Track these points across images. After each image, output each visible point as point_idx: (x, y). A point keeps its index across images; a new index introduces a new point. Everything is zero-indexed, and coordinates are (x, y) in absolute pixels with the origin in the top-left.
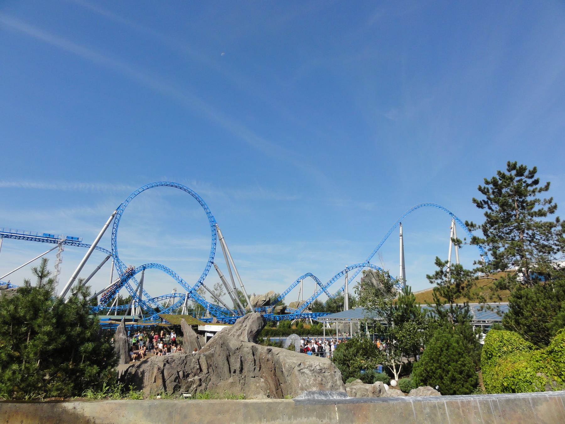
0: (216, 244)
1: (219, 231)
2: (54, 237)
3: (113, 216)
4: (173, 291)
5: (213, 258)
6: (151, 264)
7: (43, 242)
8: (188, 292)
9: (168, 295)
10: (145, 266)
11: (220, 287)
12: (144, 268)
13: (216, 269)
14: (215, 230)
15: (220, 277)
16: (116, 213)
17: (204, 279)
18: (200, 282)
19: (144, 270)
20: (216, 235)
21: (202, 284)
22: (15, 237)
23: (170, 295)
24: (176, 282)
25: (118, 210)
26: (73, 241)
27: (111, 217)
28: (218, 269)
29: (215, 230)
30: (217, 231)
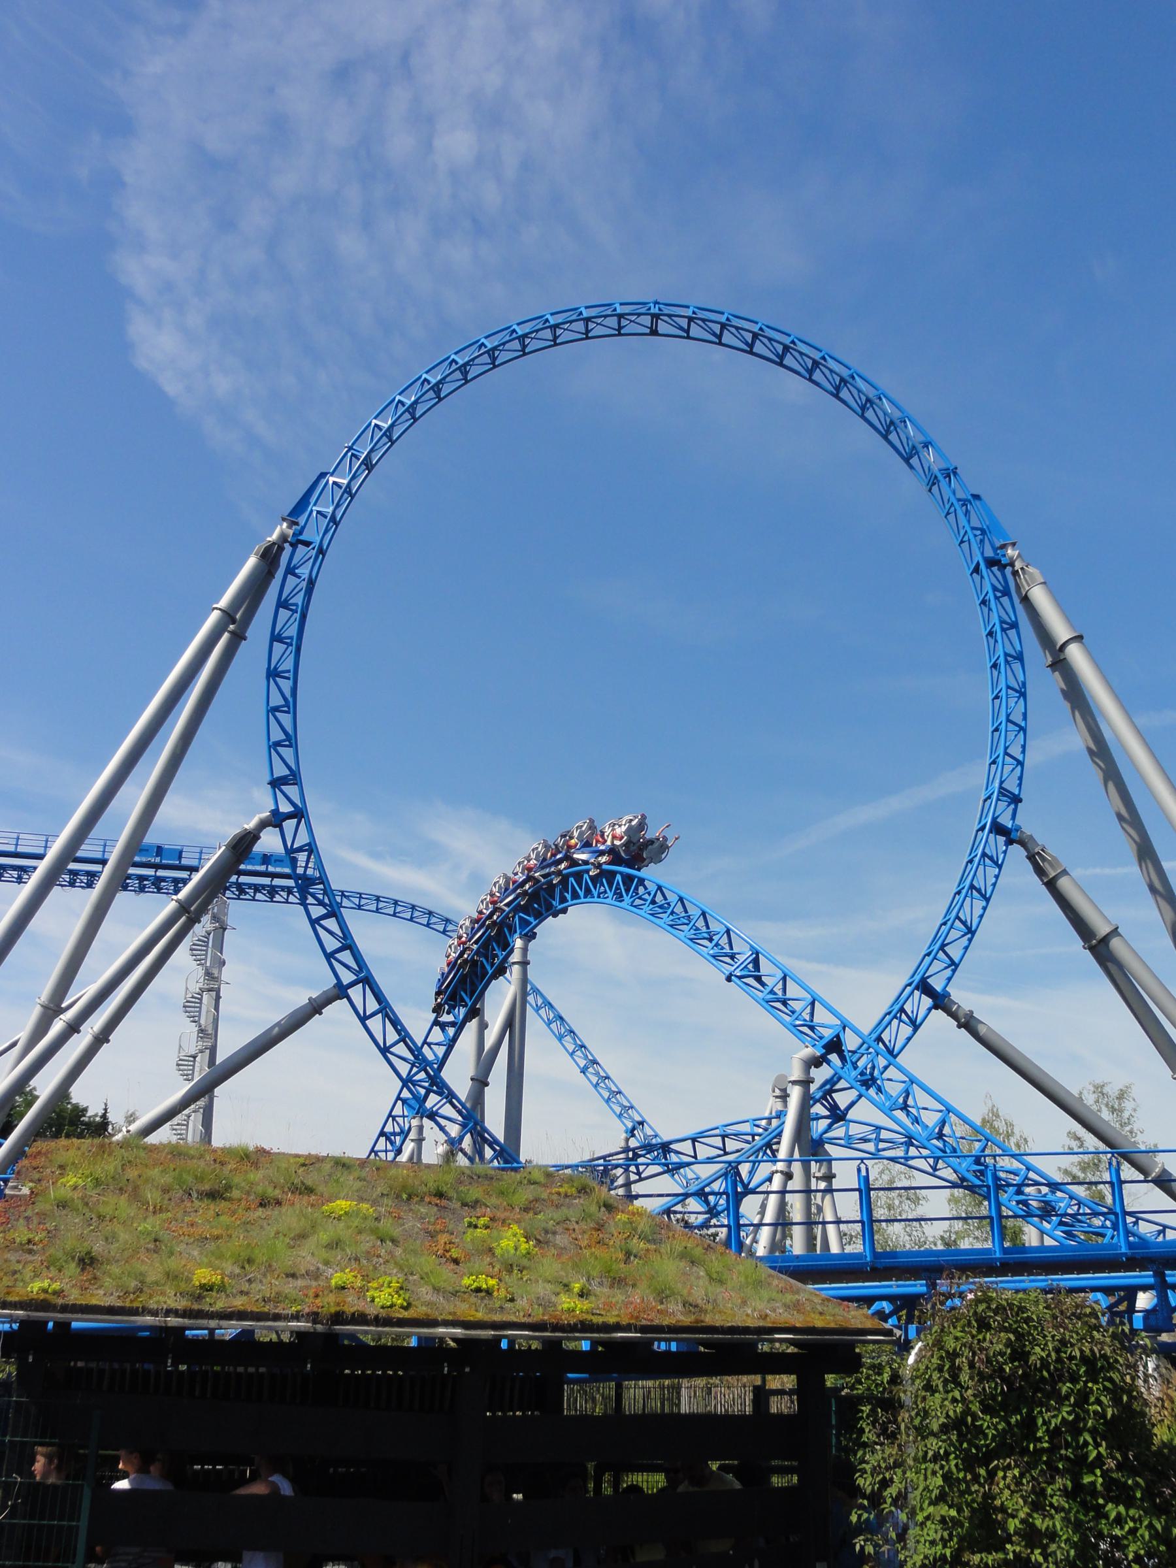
0: (1022, 694)
1: (1040, 596)
2: (184, 862)
3: (270, 557)
4: (772, 1100)
5: (1016, 800)
7: (142, 889)
8: (808, 1052)
11: (1113, 1110)
13: (1051, 885)
14: (1006, 592)
15: (1092, 949)
16: (283, 538)
17: (954, 965)
18: (925, 987)
20: (1014, 625)
21: (941, 1001)
22: (15, 874)
23: (746, 1128)
24: (712, 974)
25: (302, 520)
26: (274, 876)
27: (252, 561)
28: (1064, 884)
29: (1006, 592)
30: (1026, 600)
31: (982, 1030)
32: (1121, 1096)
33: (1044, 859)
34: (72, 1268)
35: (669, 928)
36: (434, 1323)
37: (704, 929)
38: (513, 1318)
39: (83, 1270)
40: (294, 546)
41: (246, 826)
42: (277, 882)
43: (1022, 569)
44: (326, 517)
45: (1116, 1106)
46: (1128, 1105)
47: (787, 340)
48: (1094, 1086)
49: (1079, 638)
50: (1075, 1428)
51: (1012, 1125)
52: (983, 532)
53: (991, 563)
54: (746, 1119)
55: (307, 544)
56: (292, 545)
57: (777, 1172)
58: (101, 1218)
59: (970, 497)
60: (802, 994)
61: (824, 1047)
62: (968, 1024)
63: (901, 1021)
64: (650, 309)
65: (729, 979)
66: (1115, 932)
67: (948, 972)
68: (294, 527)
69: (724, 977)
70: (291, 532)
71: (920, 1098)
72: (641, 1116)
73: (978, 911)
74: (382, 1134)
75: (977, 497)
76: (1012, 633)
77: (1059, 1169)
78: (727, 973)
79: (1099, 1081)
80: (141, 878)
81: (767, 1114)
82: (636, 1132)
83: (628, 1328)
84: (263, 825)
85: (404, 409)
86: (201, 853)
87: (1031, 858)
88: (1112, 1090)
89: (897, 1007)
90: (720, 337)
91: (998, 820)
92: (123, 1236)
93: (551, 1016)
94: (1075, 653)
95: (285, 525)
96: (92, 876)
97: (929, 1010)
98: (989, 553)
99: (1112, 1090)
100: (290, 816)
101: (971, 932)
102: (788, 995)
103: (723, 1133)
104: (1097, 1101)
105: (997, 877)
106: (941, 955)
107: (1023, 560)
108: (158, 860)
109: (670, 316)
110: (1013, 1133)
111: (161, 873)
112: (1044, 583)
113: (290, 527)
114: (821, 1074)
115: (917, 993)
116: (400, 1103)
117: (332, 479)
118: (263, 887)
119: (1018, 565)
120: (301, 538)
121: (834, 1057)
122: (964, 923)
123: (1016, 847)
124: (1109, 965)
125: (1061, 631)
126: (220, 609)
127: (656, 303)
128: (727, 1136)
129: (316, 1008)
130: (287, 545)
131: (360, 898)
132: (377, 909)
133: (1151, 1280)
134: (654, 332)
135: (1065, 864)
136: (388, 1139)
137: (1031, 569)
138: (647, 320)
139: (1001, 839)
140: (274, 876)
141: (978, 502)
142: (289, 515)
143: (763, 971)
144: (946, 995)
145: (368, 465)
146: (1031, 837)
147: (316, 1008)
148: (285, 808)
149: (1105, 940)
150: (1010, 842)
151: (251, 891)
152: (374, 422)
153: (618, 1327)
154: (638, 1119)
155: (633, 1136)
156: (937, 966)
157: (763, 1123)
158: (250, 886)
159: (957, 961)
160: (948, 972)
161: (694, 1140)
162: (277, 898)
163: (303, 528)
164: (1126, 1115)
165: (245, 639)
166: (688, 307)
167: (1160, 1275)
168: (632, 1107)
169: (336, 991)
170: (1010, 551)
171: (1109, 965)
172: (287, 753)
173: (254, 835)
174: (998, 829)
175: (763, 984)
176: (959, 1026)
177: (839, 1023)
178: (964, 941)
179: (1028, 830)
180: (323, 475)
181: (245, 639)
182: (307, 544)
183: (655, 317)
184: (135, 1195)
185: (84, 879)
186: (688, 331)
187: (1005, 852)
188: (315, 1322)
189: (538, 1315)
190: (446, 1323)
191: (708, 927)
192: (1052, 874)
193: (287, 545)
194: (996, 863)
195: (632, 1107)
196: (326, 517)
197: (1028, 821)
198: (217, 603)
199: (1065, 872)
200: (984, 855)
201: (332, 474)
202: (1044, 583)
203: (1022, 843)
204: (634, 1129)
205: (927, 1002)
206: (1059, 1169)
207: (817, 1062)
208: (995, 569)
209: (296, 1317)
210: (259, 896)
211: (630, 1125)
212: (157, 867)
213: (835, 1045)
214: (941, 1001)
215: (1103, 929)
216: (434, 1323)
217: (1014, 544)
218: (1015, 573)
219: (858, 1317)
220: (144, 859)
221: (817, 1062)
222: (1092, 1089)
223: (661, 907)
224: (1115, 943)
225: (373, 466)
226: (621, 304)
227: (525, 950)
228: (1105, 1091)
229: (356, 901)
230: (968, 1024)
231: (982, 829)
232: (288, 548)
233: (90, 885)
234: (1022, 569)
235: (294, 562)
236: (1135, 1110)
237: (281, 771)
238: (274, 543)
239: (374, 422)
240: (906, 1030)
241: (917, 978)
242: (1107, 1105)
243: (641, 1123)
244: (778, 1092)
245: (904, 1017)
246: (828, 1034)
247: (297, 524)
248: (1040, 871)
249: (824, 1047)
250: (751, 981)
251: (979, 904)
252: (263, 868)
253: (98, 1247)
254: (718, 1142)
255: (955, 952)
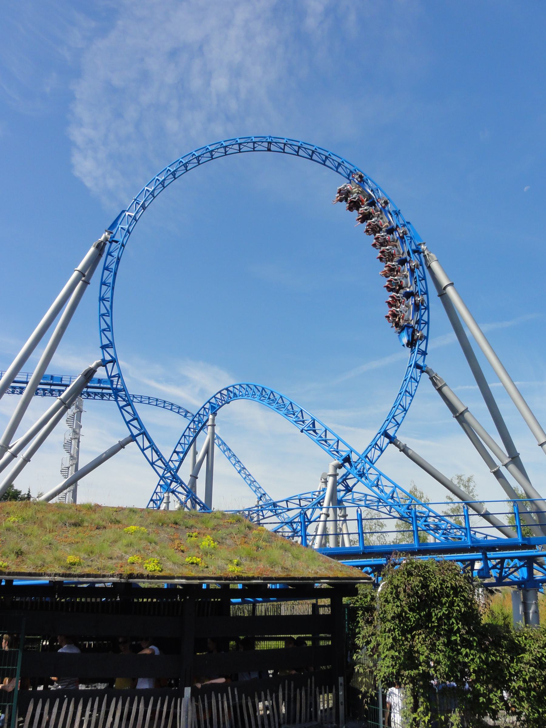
1: (435, 266)
2: (63, 382)
3: (100, 248)
4: (320, 483)
6: (227, 389)
7: (44, 395)
8: (336, 462)
9: (302, 497)
10: (213, 401)
11: (465, 486)
12: (214, 410)
13: (440, 390)
15: (457, 417)
16: (106, 239)
17: (398, 425)
18: (386, 435)
19: (215, 414)
20: (424, 279)
21: (392, 440)
23: (309, 496)
25: (114, 231)
26: (103, 388)
27: (92, 249)
28: (445, 390)
30: (429, 268)
31: (410, 452)
32: (469, 480)
33: (436, 379)
34: (13, 556)
35: (276, 410)
36: (173, 578)
37: (291, 410)
38: (208, 575)
39: (17, 557)
40: (111, 242)
41: (91, 366)
42: (104, 391)
43: (428, 254)
44: (125, 230)
45: (467, 485)
46: (472, 484)
47: (327, 154)
48: (458, 476)
49: (452, 284)
50: (448, 617)
51: (422, 493)
52: (411, 238)
53: (414, 252)
54: (309, 492)
55: (117, 242)
56: (110, 242)
57: (322, 514)
58: (26, 535)
59: (406, 223)
60: (334, 438)
61: (343, 460)
62: (404, 450)
63: (375, 449)
64: (267, 140)
65: (302, 431)
66: (466, 410)
67: (396, 428)
68: (111, 234)
69: (300, 430)
70: (109, 237)
71: (384, 482)
72: (264, 491)
73: (408, 401)
74: (152, 500)
75: (408, 223)
76: (423, 282)
77: (443, 512)
78: (301, 429)
79: (459, 474)
80: (44, 390)
81: (318, 490)
82: (262, 498)
83: (258, 578)
84: (98, 365)
85: (159, 183)
86: (71, 379)
87: (431, 379)
88: (465, 478)
89: (374, 443)
90: (298, 152)
91: (418, 362)
92: (36, 542)
93: (225, 449)
94: (450, 291)
95: (107, 233)
96: (22, 389)
97: (388, 444)
98: (414, 247)
99: (465, 478)
100: (110, 362)
101: (405, 410)
102: (327, 438)
103: (299, 498)
104: (459, 483)
105: (417, 387)
106: (393, 420)
107: (428, 251)
108: (51, 382)
109: (276, 143)
110: (423, 497)
111: (53, 387)
112: (437, 260)
113: (109, 234)
114: (341, 472)
115: (382, 437)
116: (159, 486)
117: (127, 213)
118: (99, 393)
119: (426, 253)
120: (114, 239)
121: (347, 464)
122: (402, 407)
123: (425, 375)
124: (464, 424)
125: (444, 281)
126: (78, 271)
127: (270, 137)
128: (301, 499)
129: (122, 445)
130: (108, 242)
131: (141, 398)
132: (149, 403)
133: (481, 557)
134: (269, 150)
135: (445, 381)
136: (154, 502)
137: (431, 254)
138: (266, 145)
139: (419, 371)
140: (103, 388)
141: (408, 226)
142: (108, 229)
143: (316, 428)
144: (395, 437)
145: (144, 207)
146: (431, 369)
147: (122, 445)
148: (108, 358)
149: (462, 414)
150: (422, 372)
151: (93, 395)
152: (146, 188)
153: (253, 578)
154: (263, 492)
155: (261, 500)
156: (391, 425)
157: (317, 493)
158: (93, 393)
159: (399, 423)
160: (396, 428)
161: (287, 501)
162: (105, 398)
163: (115, 235)
164: (471, 488)
165: (89, 284)
166: (284, 139)
167: (485, 554)
168: (260, 488)
169: (131, 438)
170: (422, 247)
171: (464, 424)
172: (108, 334)
173: (94, 370)
174: (417, 366)
175: (317, 433)
176: (400, 451)
177: (349, 450)
178: (403, 414)
179: (430, 367)
180: (123, 211)
181: (89, 284)
182: (117, 242)
183: (270, 143)
184: (41, 525)
185: (19, 390)
186: (284, 150)
187: (420, 376)
188: (121, 578)
189: (219, 574)
190: (179, 578)
191: (293, 409)
192: (440, 385)
193: (108, 242)
194: (416, 381)
195: (260, 488)
196: (125, 230)
197: (430, 362)
198: (77, 267)
199: (445, 385)
200: (411, 377)
201: (127, 211)
202: (437, 260)
203: (427, 372)
204: (261, 497)
205: (387, 440)
206: (443, 512)
207: (340, 466)
208: (416, 254)
209: (112, 576)
210: (97, 397)
211: (259, 495)
212: (51, 385)
213: (347, 459)
214: (392, 440)
215: (461, 409)
216: (173, 578)
217: (424, 243)
218: (425, 256)
219: (356, 573)
220: (45, 381)
221: (340, 466)
222: (457, 478)
223: (272, 400)
224: (466, 415)
225: (146, 208)
226: (255, 137)
227: (213, 420)
228: (462, 478)
229: (140, 399)
230: (404, 450)
231: (411, 366)
232: (108, 244)
233: (21, 393)
234: (428, 254)
235: (111, 250)
236: (474, 486)
237: (105, 342)
238: (102, 242)
239: (146, 188)
240: (378, 453)
241: (383, 430)
242: (463, 484)
243: (264, 494)
244: (323, 480)
245: (377, 447)
246: (344, 454)
247: (112, 233)
248: (435, 384)
249: (343, 460)
250: (311, 432)
251: (409, 398)
252: (98, 385)
253: (24, 547)
254: (297, 502)
255: (399, 419)
